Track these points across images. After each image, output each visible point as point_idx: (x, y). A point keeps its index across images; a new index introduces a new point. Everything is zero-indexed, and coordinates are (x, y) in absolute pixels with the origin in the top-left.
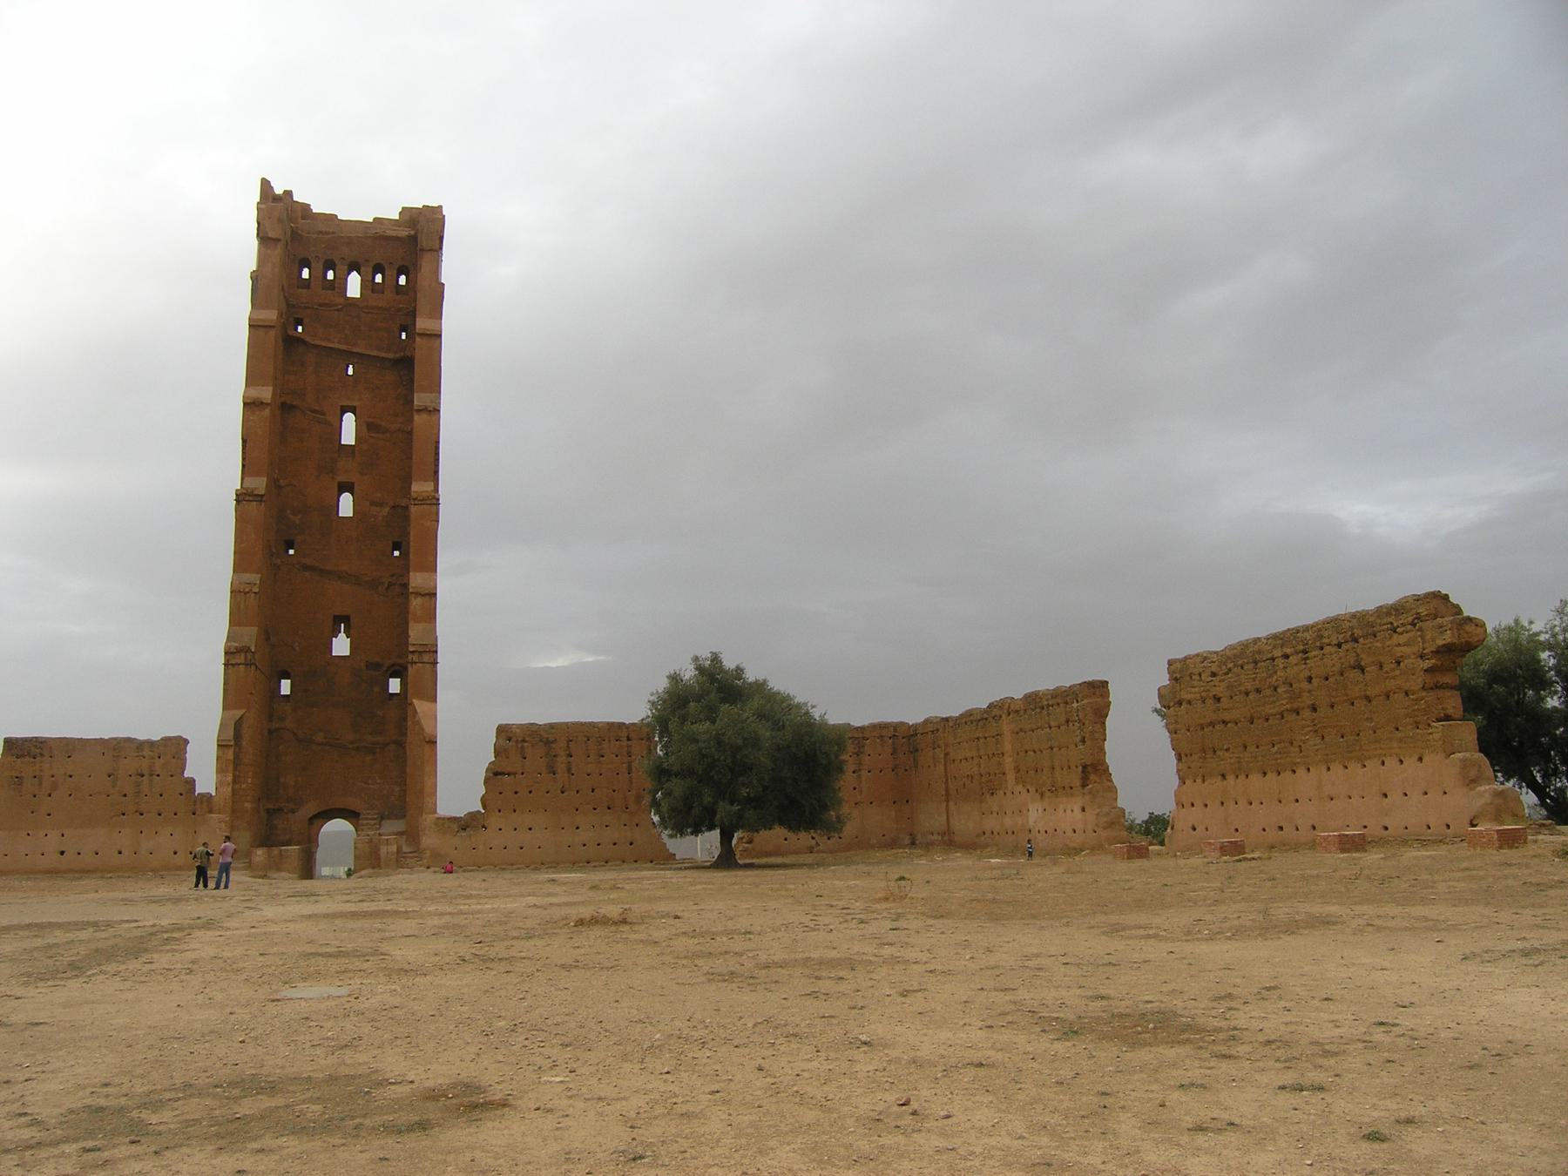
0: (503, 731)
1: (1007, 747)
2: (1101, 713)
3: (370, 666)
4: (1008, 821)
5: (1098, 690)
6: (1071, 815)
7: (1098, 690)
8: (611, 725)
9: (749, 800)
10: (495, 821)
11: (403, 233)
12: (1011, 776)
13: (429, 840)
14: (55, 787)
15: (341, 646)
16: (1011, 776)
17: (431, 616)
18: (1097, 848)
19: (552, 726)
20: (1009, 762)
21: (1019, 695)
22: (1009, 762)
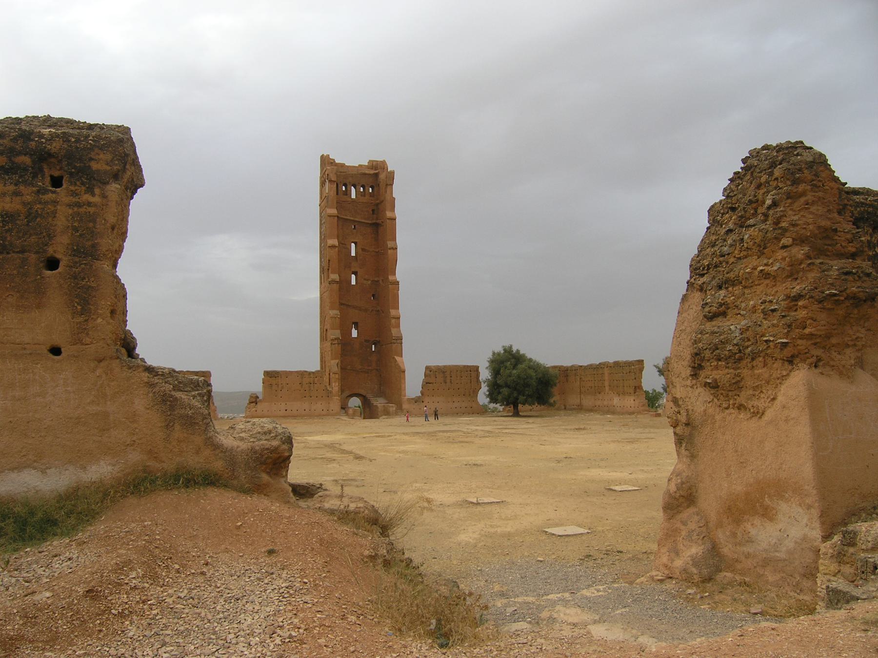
0: (427, 368)
1: (606, 377)
2: (641, 370)
3: (366, 341)
4: (605, 403)
5: (641, 362)
6: (630, 402)
7: (641, 362)
8: (465, 366)
9: (529, 396)
10: (426, 399)
11: (372, 172)
12: (607, 388)
13: (405, 406)
14: (283, 388)
15: (354, 333)
16: (607, 388)
17: (398, 326)
18: (639, 413)
19: (445, 366)
20: (607, 384)
21: (611, 361)
22: (607, 384)
